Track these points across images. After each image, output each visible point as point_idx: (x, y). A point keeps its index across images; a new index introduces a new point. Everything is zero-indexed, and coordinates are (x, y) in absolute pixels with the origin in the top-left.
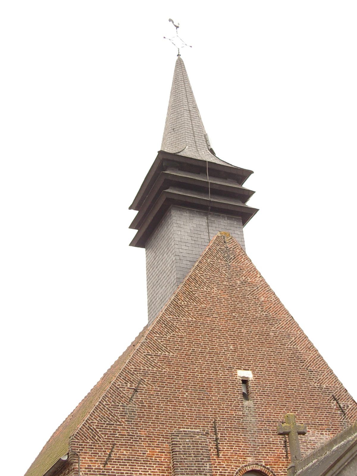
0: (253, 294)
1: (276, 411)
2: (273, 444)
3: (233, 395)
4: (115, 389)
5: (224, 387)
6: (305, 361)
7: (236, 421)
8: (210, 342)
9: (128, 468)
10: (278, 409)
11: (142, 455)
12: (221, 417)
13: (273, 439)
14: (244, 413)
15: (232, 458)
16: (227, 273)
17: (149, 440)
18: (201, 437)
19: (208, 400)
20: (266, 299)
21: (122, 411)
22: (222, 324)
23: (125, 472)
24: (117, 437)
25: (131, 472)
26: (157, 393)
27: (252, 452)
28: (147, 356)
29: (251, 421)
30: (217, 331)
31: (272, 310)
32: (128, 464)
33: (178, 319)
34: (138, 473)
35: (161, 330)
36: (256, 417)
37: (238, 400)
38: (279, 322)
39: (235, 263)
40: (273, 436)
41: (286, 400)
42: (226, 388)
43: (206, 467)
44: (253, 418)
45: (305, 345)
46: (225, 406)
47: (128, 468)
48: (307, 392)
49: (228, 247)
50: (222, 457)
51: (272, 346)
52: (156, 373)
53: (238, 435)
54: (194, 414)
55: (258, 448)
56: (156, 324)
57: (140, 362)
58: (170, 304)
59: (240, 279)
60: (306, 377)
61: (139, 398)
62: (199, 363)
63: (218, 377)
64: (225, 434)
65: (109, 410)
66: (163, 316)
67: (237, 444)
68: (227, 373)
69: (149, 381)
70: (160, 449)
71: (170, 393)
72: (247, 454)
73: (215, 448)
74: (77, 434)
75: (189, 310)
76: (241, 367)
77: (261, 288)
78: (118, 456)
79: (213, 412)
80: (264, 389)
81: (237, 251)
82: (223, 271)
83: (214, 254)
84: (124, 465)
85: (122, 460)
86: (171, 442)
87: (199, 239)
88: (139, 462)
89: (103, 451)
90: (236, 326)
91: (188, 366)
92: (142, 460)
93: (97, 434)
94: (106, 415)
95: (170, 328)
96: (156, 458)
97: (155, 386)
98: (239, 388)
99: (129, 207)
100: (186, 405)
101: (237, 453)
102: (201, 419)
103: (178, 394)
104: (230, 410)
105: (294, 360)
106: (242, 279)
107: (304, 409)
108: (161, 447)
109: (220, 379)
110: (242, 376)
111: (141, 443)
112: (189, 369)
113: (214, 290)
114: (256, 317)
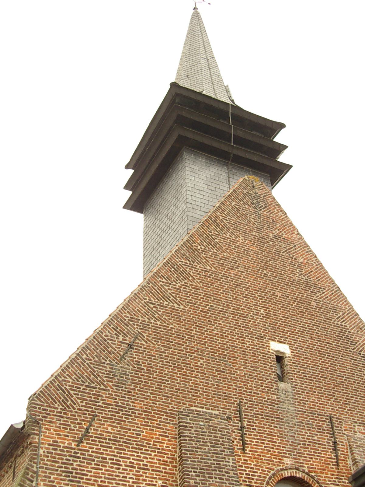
0: (289, 252)
1: (322, 401)
2: (319, 444)
3: (265, 372)
4: (101, 340)
5: (252, 359)
6: (356, 343)
7: (269, 407)
8: (234, 300)
9: (114, 452)
10: (324, 399)
11: (135, 435)
12: (248, 399)
13: (318, 438)
14: (279, 398)
15: (263, 456)
16: (256, 222)
17: (146, 417)
18: (221, 422)
19: (232, 374)
20: (306, 261)
21: (109, 372)
22: (250, 281)
23: (108, 457)
24: (99, 406)
25: (118, 458)
26: (159, 355)
27: (290, 451)
28: (148, 304)
29: (289, 409)
30: (244, 289)
31: (313, 276)
32: (114, 447)
33: (192, 265)
34: (128, 461)
35: (169, 274)
36: (296, 405)
37: (271, 379)
38: (322, 291)
39: (267, 213)
40: (319, 434)
41: (335, 388)
42: (255, 362)
43: (229, 462)
44: (292, 407)
45: (356, 324)
46: (253, 385)
47: (114, 452)
48: (361, 383)
49: (257, 193)
50: (249, 454)
51: (314, 318)
52: (160, 328)
53: (271, 426)
54: (211, 389)
55: (299, 447)
56: (162, 266)
57: (138, 310)
58: (182, 245)
59: (273, 232)
60: (358, 363)
61: (135, 358)
62: (219, 324)
63: (244, 346)
64: (253, 422)
65: (90, 366)
66: (173, 257)
67: (270, 438)
68: (256, 343)
69: (150, 337)
70: (161, 430)
71: (178, 357)
72: (284, 453)
73: (239, 439)
74: (40, 393)
75: (207, 257)
76: (274, 338)
77: (299, 247)
78: (99, 432)
79: (238, 391)
80: (305, 371)
81: (269, 200)
82: (251, 219)
83: (240, 197)
84: (107, 447)
85: (105, 439)
86: (177, 423)
87: (217, 190)
88: (131, 446)
89: (78, 423)
90: (269, 287)
91: (204, 325)
92: (135, 443)
93: (70, 398)
94: (86, 374)
95: (181, 275)
96: (155, 443)
97: (158, 345)
98: (272, 365)
99: (126, 166)
100: (201, 376)
101: (270, 451)
102: (220, 398)
103: (189, 360)
104: (260, 391)
105: (342, 339)
106: (276, 232)
107: (358, 404)
108: (163, 429)
109: (247, 349)
110: (276, 350)
111: (135, 420)
112: (205, 329)
113: (240, 239)
114: (293, 280)
